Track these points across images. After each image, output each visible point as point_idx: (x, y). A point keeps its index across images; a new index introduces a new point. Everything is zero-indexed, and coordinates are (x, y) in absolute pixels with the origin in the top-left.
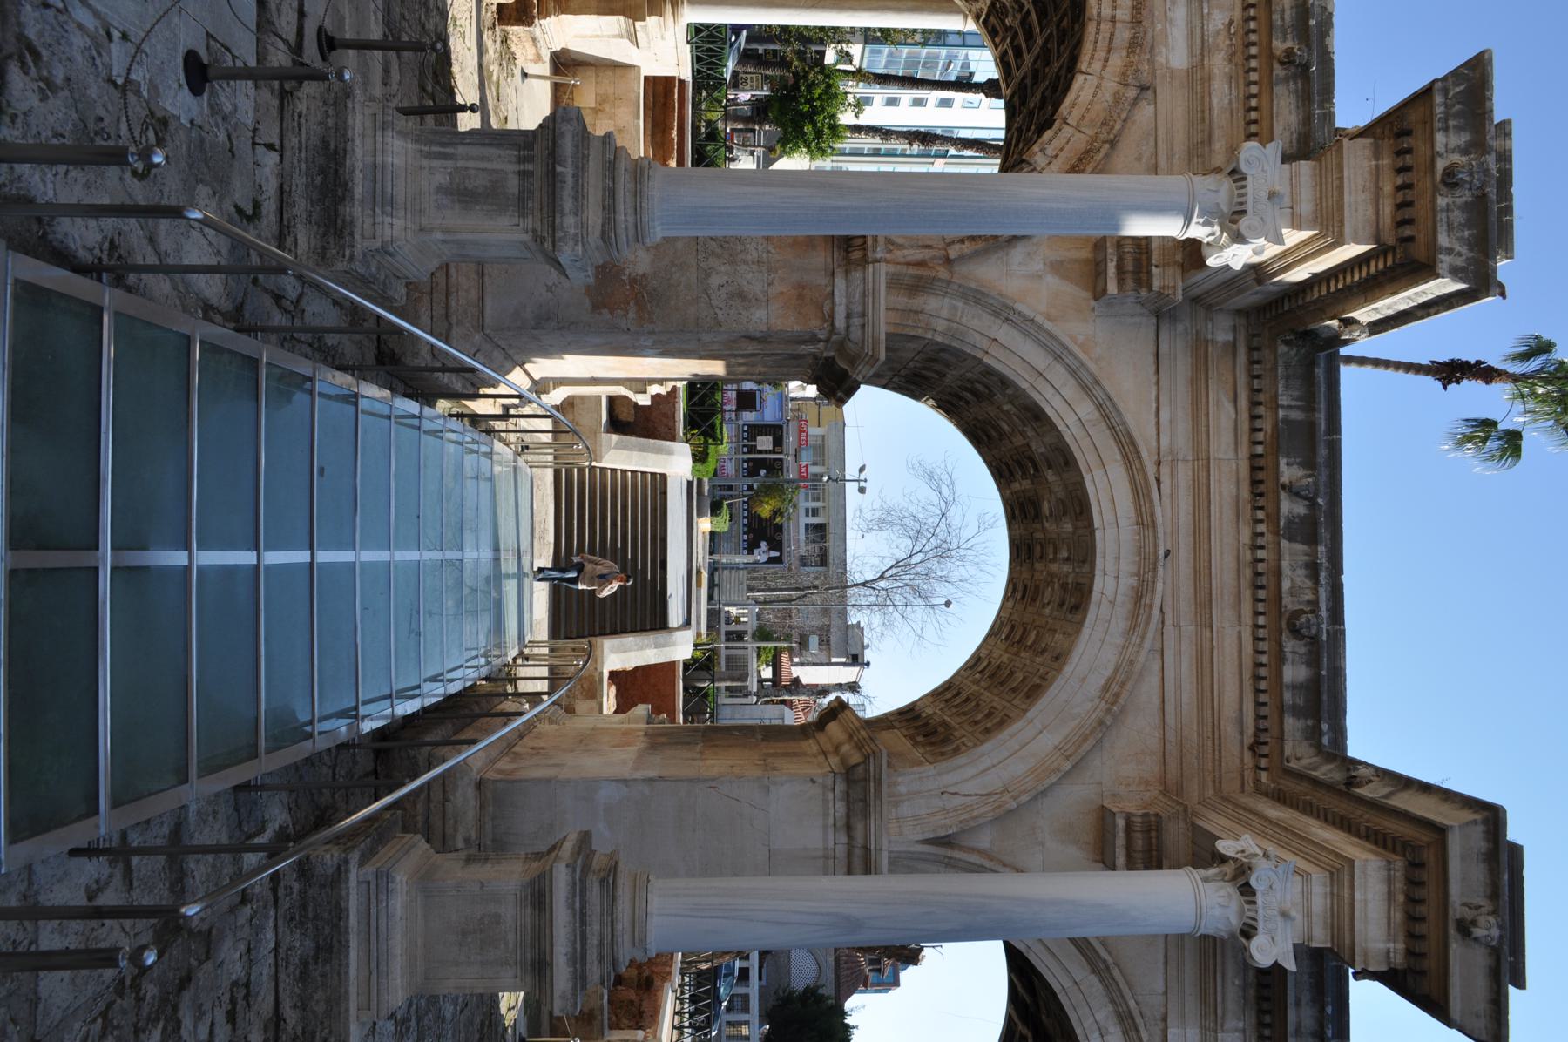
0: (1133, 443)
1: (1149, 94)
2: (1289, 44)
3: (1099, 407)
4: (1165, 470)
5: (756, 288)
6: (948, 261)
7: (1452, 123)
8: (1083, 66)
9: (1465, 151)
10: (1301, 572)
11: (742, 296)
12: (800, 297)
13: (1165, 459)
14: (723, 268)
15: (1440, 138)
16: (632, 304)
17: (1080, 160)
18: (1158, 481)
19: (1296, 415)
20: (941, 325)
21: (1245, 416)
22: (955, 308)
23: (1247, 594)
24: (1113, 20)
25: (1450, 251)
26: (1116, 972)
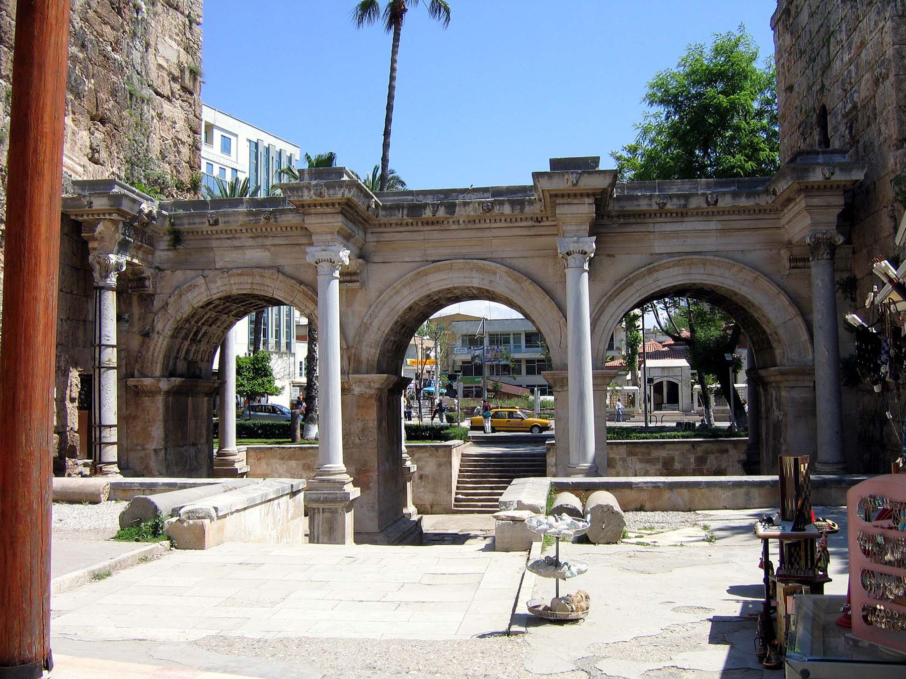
0: (419, 273)
1: (280, 268)
2: (262, 218)
3: (404, 286)
4: (429, 259)
5: (360, 424)
6: (348, 347)
7: (300, 194)
8: (270, 295)
9: (310, 190)
10: (467, 208)
11: (363, 430)
12: (363, 407)
13: (425, 258)
14: (353, 438)
15: (305, 198)
16: (367, 474)
17: (307, 296)
18: (434, 262)
19: (405, 212)
20: (373, 351)
21: (407, 228)
22: (366, 345)
23: (478, 226)
24: (252, 283)
25: (343, 194)
26: (631, 276)
